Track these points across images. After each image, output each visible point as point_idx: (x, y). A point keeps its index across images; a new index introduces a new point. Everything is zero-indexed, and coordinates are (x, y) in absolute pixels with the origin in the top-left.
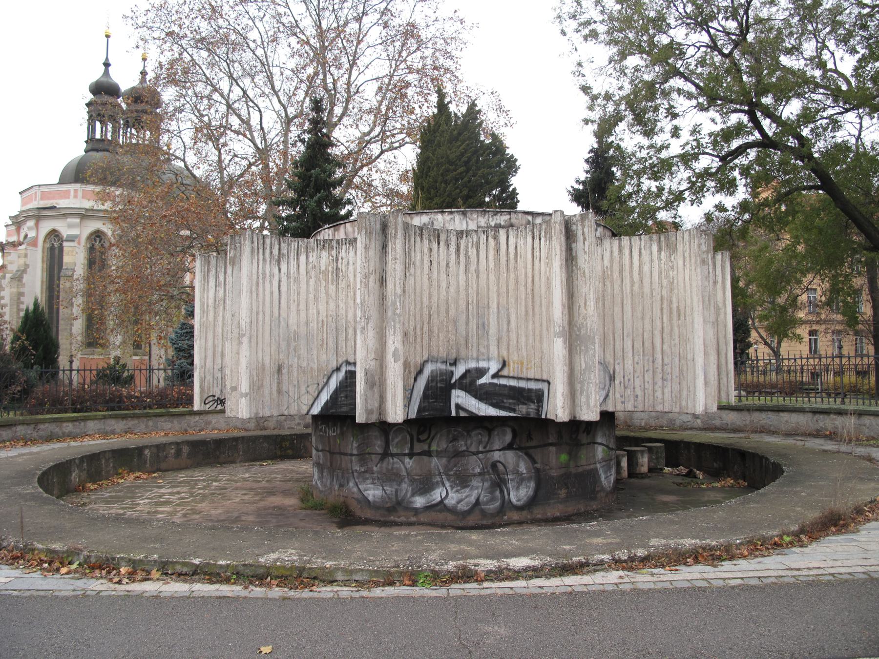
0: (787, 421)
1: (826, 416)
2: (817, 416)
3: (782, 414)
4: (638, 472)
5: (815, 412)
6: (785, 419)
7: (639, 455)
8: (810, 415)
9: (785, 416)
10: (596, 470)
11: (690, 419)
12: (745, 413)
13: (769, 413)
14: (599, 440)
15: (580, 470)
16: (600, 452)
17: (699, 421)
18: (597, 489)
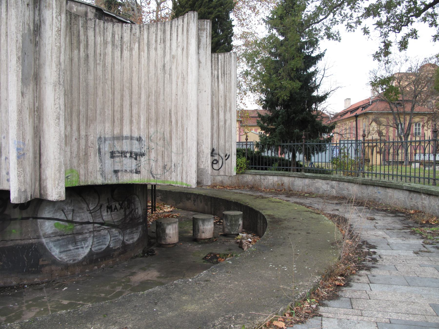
0: (391, 197)
1: (418, 195)
2: (412, 194)
3: (389, 190)
4: (199, 237)
5: (411, 191)
6: (390, 194)
7: (200, 223)
8: (407, 193)
9: (390, 192)
10: (42, 244)
12: (364, 187)
13: (379, 188)
14: (46, 214)
15: (10, 244)
16: (48, 227)
18: (41, 263)
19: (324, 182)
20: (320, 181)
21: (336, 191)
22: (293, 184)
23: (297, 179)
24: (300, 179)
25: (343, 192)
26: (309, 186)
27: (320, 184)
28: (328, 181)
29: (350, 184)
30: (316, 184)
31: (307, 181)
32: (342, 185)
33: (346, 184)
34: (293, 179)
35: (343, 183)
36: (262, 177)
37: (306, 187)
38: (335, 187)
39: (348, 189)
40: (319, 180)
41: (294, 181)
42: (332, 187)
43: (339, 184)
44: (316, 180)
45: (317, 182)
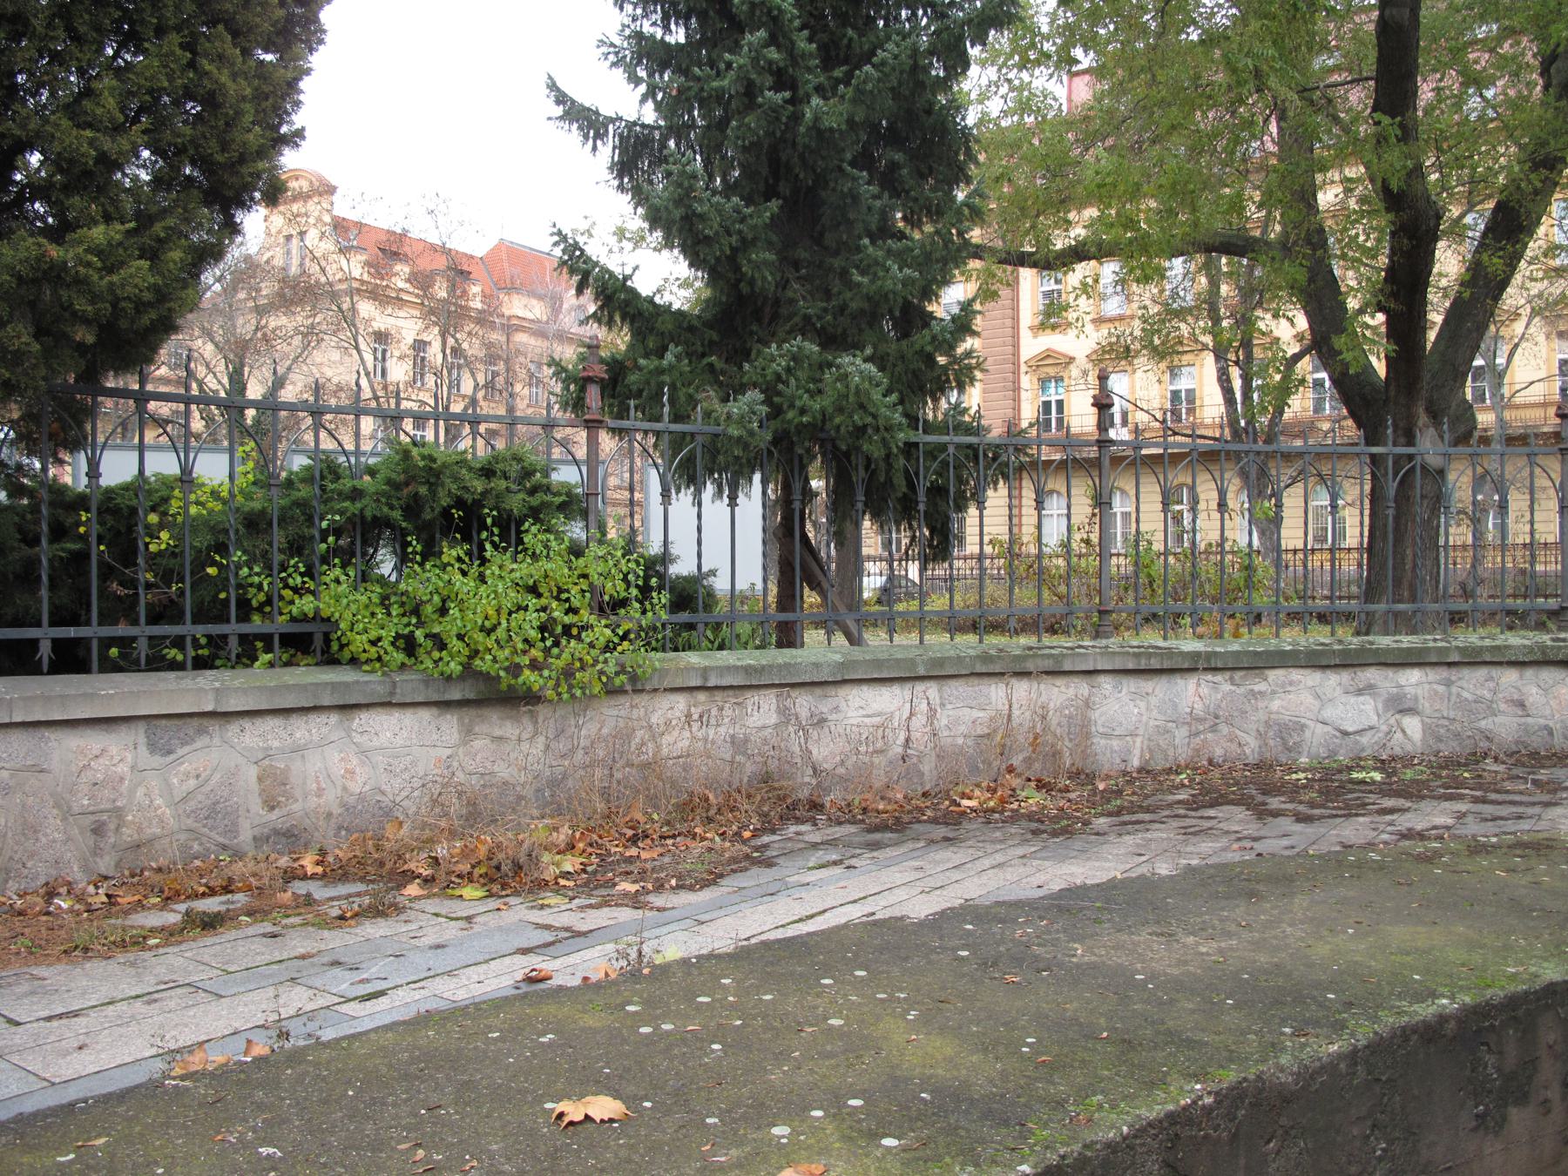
11: (1374, 720)
17: (1413, 725)
19: (1333, 681)
20: (1311, 678)
21: (1426, 729)
22: (1082, 729)
23: (1106, 683)
24: (1131, 684)
25: (1483, 724)
26: (1214, 720)
27: (1308, 699)
28: (1372, 675)
29: (1529, 673)
30: (1276, 705)
31: (1192, 692)
32: (1472, 682)
33: (1510, 677)
34: (1080, 687)
35: (1482, 672)
36: (803, 703)
37: (1181, 734)
38: (1424, 705)
39: (1521, 704)
40: (1295, 675)
41: (1088, 704)
42: (1401, 706)
43: (1448, 683)
44: (1273, 675)
45: (1285, 688)
